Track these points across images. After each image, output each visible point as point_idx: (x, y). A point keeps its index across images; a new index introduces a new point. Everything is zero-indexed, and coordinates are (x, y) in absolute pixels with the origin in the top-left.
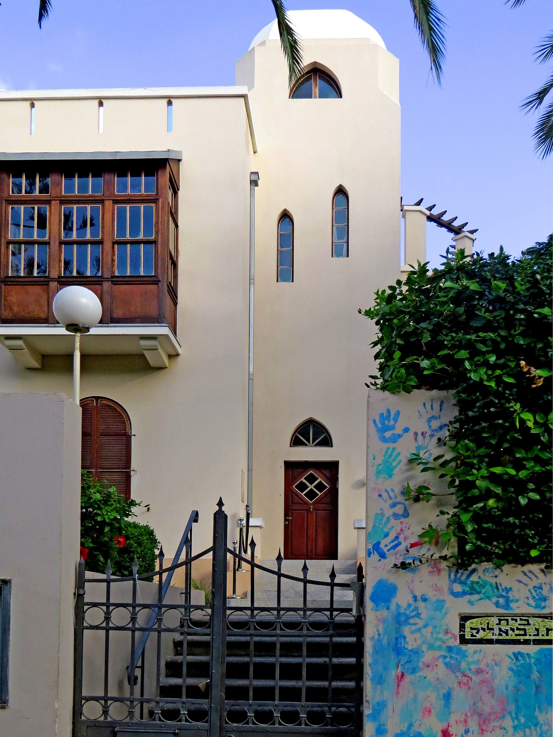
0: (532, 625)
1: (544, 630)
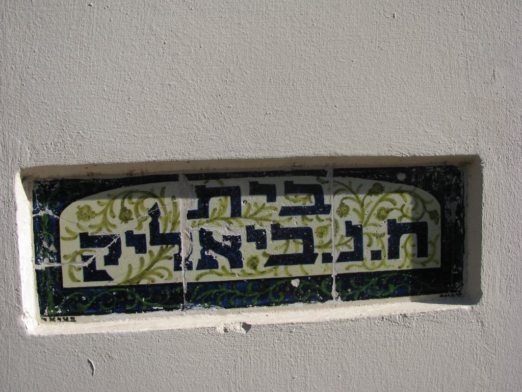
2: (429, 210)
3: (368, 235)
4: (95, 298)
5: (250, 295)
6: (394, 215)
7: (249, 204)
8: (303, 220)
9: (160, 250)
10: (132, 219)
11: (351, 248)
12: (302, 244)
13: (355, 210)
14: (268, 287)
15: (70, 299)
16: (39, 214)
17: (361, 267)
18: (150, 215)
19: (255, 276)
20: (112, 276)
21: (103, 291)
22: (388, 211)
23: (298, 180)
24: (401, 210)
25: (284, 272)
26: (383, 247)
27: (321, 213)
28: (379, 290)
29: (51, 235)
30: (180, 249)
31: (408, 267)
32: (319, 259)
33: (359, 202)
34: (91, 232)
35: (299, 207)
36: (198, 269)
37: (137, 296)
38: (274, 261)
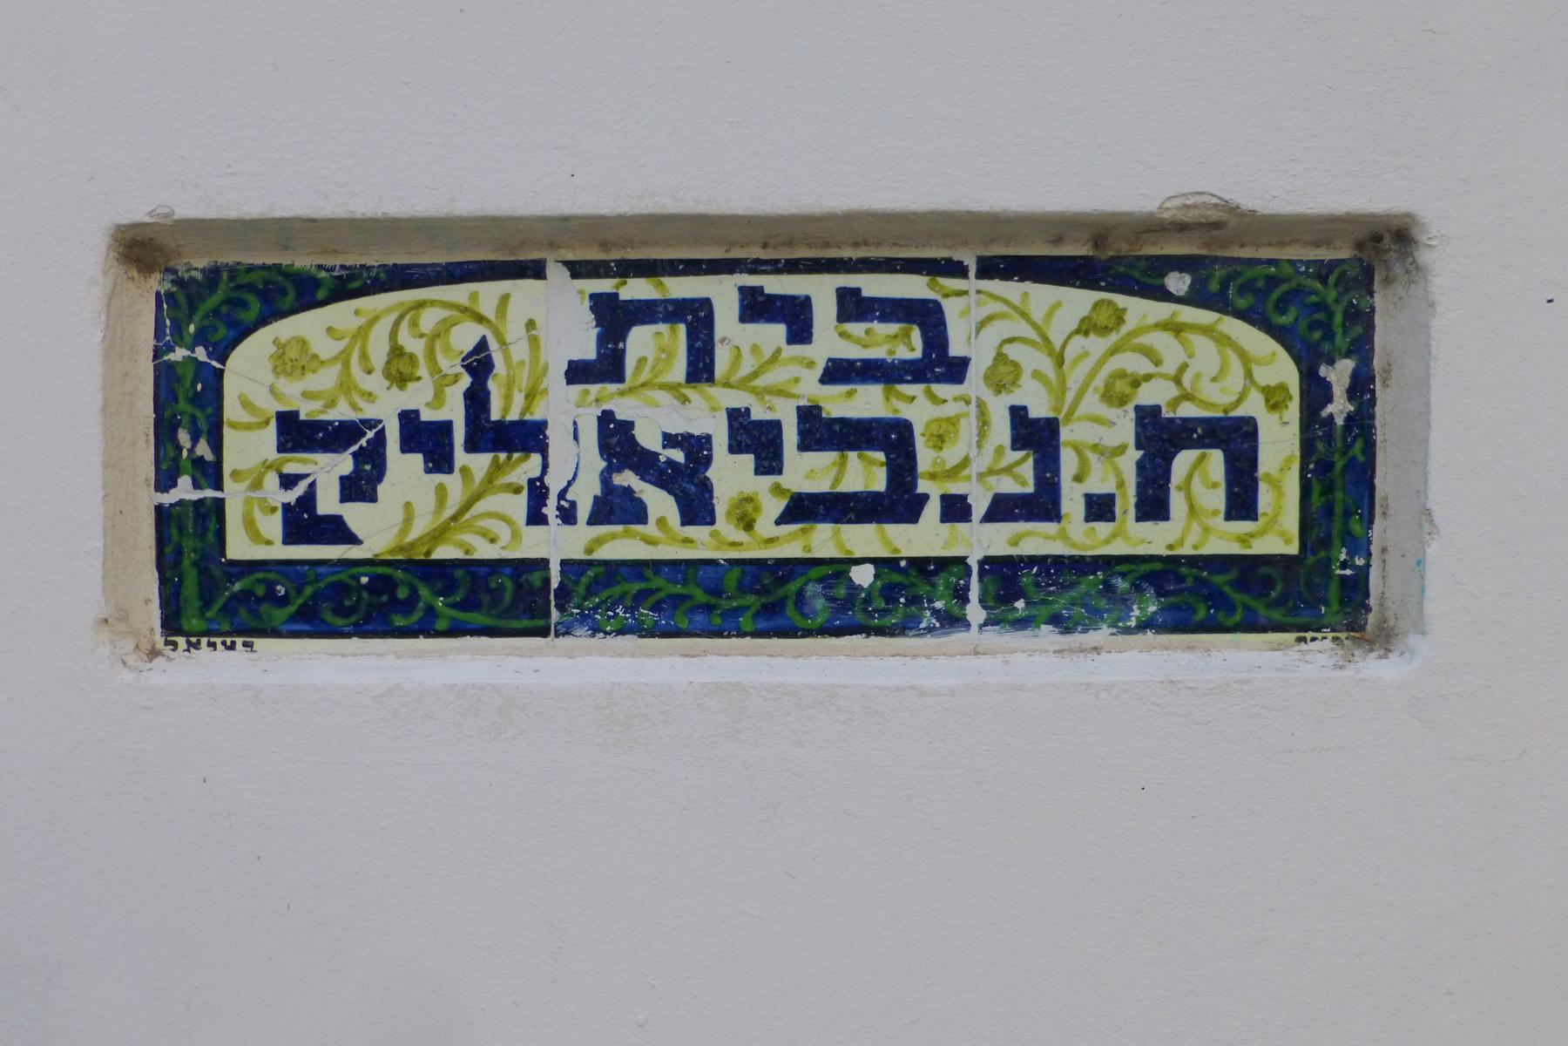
0: (975, 373)
3: (1078, 449)
4: (308, 591)
5: (735, 604)
6: (1155, 394)
7: (738, 348)
8: (888, 399)
9: (490, 467)
10: (419, 379)
11: (1024, 483)
12: (882, 464)
13: (1037, 374)
14: (784, 581)
15: (242, 591)
16: (172, 357)
18: (469, 368)
19: (749, 549)
21: (333, 573)
22: (1136, 383)
23: (874, 286)
24: (1177, 380)
29: (199, 414)
30: (545, 466)
31: (1195, 547)
32: (933, 509)
34: (307, 411)
35: (876, 361)
36: (590, 522)
37: (424, 591)
38: (802, 509)
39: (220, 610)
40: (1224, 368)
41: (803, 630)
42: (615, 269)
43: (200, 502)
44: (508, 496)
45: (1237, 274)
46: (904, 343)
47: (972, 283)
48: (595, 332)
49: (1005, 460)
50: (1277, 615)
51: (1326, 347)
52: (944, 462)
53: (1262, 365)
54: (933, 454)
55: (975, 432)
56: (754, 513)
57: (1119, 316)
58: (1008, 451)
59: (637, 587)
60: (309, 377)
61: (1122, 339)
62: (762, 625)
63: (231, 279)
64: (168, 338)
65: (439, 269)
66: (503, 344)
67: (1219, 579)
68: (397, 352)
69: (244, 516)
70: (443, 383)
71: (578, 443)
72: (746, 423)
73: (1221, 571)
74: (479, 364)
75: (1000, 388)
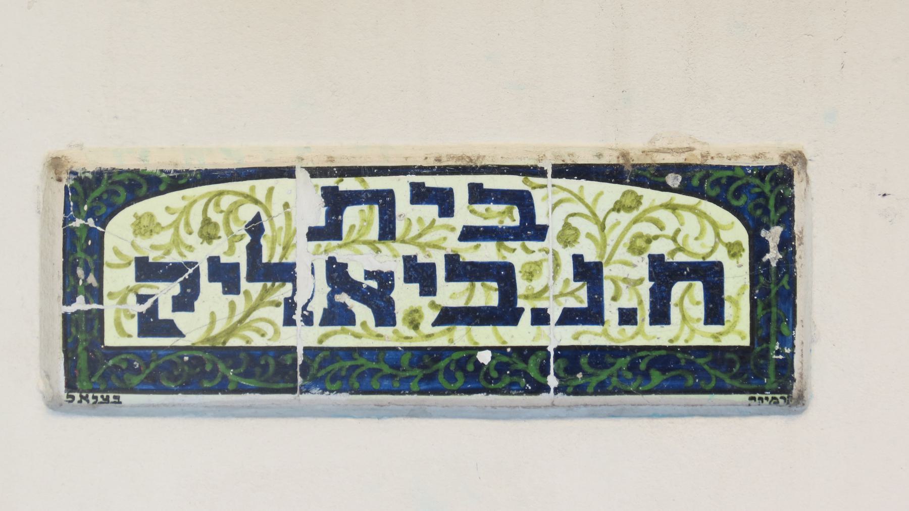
0: (551, 234)
1: (634, 274)
2: (726, 241)
3: (614, 281)
4: (152, 366)
5: (408, 374)
6: (660, 247)
8: (499, 250)
9: (261, 291)
10: (220, 237)
11: (581, 302)
13: (589, 236)
14: (437, 360)
16: (73, 224)
17: (600, 335)
18: (249, 231)
19: (416, 341)
20: (184, 332)
22: (649, 241)
23: (491, 182)
24: (674, 239)
25: (465, 338)
26: (640, 302)
27: (530, 239)
28: (634, 379)
29: (89, 259)
30: (295, 290)
31: (686, 341)
32: (526, 317)
33: (597, 222)
34: (154, 256)
35: (492, 227)
36: (323, 323)
37: (221, 367)
39: (100, 376)
40: (702, 232)
41: (450, 390)
42: (336, 172)
43: (90, 311)
44: (273, 308)
45: (707, 176)
46: (509, 217)
47: (549, 180)
48: (324, 210)
49: (569, 288)
50: (736, 384)
51: (765, 219)
52: (533, 288)
53: (725, 230)
54: (527, 283)
55: (552, 270)
56: (419, 319)
57: (638, 200)
58: (572, 282)
59: (349, 364)
60: (155, 236)
61: (640, 214)
62: (424, 387)
63: (110, 178)
64: (72, 213)
65: (232, 172)
66: (270, 217)
67: (701, 361)
68: (207, 222)
69: (115, 320)
70: (234, 240)
71: (314, 276)
72: (414, 264)
73: (704, 356)
74: (256, 228)
75: (566, 244)
